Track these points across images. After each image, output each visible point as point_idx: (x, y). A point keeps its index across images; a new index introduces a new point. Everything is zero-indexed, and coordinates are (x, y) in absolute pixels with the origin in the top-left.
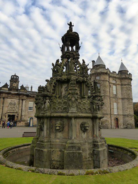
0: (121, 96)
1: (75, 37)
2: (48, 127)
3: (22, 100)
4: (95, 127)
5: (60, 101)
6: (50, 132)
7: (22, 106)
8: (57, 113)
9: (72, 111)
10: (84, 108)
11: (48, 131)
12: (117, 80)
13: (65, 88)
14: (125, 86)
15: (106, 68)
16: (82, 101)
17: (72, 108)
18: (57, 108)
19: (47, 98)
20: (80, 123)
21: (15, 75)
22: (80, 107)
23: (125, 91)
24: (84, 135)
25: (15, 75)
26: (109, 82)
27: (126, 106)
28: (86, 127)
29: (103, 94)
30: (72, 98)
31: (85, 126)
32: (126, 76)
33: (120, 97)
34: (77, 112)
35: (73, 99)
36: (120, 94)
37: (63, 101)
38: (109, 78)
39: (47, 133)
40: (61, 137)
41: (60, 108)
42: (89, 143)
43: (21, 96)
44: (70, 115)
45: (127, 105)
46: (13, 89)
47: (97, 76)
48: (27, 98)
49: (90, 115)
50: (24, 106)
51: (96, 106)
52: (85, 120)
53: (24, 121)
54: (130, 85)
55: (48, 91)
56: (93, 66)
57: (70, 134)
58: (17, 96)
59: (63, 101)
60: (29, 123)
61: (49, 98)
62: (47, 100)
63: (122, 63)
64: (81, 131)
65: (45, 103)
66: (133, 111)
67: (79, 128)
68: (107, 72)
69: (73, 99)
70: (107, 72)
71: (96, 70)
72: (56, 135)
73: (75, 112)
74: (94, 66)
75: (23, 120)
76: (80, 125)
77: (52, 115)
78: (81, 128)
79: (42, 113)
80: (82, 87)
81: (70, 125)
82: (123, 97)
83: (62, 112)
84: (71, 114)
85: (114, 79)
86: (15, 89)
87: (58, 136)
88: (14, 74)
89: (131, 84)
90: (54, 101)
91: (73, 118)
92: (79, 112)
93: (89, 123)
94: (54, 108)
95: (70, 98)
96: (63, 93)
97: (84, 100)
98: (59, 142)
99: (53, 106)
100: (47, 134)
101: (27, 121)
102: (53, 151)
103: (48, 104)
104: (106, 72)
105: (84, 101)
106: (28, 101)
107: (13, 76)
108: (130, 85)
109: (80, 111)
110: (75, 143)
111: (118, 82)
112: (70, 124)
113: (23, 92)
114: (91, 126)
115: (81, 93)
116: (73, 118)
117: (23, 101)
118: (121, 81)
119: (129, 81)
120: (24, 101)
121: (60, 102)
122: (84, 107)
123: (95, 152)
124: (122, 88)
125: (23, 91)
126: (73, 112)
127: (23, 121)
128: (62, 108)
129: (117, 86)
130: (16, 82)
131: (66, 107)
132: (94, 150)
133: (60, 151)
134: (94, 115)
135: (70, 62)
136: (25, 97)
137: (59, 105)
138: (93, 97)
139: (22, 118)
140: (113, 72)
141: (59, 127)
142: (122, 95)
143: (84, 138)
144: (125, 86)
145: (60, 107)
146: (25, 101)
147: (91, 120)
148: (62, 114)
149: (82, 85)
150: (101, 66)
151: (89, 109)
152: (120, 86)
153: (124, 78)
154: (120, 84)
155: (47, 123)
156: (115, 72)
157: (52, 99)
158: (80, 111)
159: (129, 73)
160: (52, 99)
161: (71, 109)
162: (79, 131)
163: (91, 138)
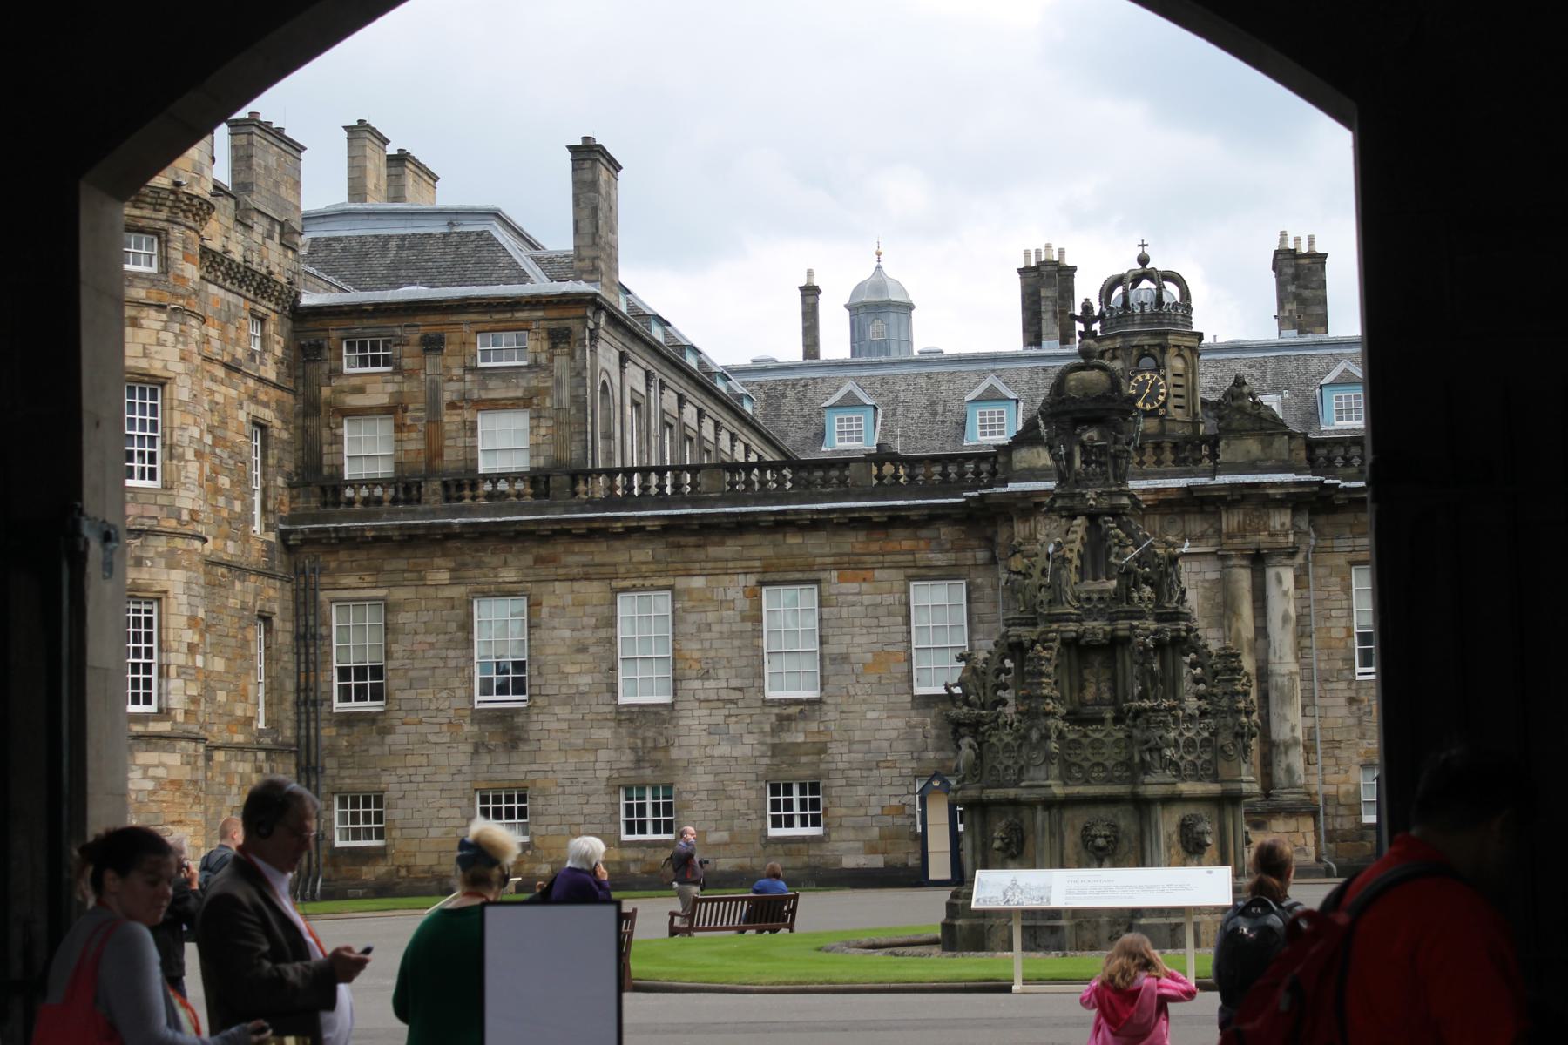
1: (1091, 406)
2: (978, 843)
3: (1258, 561)
4: (1148, 835)
7: (1262, 631)
8: (1000, 786)
9: (1032, 780)
10: (1098, 764)
16: (1086, 735)
18: (1001, 768)
19: (962, 730)
20: (1079, 825)
21: (1143, 260)
22: (1077, 760)
25: (1143, 260)
28: (1096, 836)
31: (1093, 832)
43: (1231, 521)
44: (1024, 794)
46: (1141, 449)
48: (1320, 534)
50: (1282, 639)
51: (1141, 752)
52: (1103, 812)
53: (1307, 809)
58: (1196, 525)
60: (1370, 826)
61: (973, 730)
62: (963, 737)
67: (1076, 845)
75: (1289, 798)
76: (1078, 833)
77: (984, 797)
80: (1119, 665)
84: (1029, 791)
86: (1158, 447)
88: (1129, 264)
90: (994, 740)
91: (1039, 807)
92: (1078, 779)
95: (1022, 731)
97: (1097, 730)
101: (1355, 808)
102: (992, 926)
105: (1098, 736)
106: (1341, 560)
107: (1118, 281)
109: (1079, 775)
113: (1253, 467)
114: (1133, 836)
115: (1114, 690)
116: (1039, 807)
117: (1271, 573)
120: (1282, 579)
122: (1098, 759)
125: (1252, 446)
126: (1036, 783)
127: (1292, 812)
130: (1163, 349)
136: (1280, 520)
137: (1007, 755)
139: (1279, 774)
141: (1002, 839)
146: (1288, 576)
147: (1130, 808)
149: (1118, 655)
151: (1122, 763)
157: (983, 734)
158: (1079, 775)
160: (983, 734)
161: (1028, 771)
162: (1078, 854)
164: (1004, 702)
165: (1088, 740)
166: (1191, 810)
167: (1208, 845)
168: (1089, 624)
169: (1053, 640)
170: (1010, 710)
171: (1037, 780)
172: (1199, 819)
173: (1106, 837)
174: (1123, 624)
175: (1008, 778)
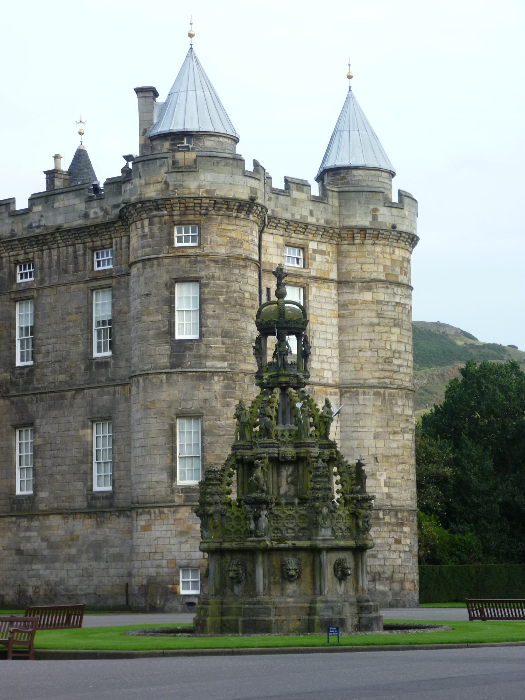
0: (335, 367)
5: (292, 513)
6: (270, 583)
9: (323, 536)
11: (267, 582)
12: (313, 246)
13: (288, 476)
14: (369, 289)
15: (249, 167)
17: (323, 530)
18: (283, 529)
23: (363, 333)
24: (341, 589)
26: (258, 264)
27: (370, 442)
29: (224, 359)
30: (322, 508)
32: (375, 218)
33: (329, 377)
34: (333, 538)
35: (325, 511)
36: (328, 352)
37: (297, 512)
38: (261, 232)
39: (264, 584)
40: (295, 592)
41: (290, 528)
42: (351, 604)
45: (376, 437)
47: (180, 223)
49: (351, 543)
54: (399, 285)
55: (263, 491)
56: (144, 132)
57: (318, 583)
59: (297, 512)
63: (349, 98)
64: (336, 579)
65: (257, 518)
66: (413, 477)
68: (253, 199)
69: (325, 511)
70: (253, 199)
71: (172, 179)
72: (282, 589)
73: (328, 537)
74: (152, 139)
76: (333, 566)
78: (335, 570)
79: (252, 541)
81: (317, 565)
82: (347, 376)
83: (296, 538)
85: (296, 238)
87: (289, 591)
89: (406, 273)
90: (276, 512)
91: (325, 552)
93: (349, 559)
94: (277, 529)
96: (284, 489)
98: (294, 602)
99: (272, 524)
100: (264, 589)
103: (264, 522)
104: (244, 195)
108: (399, 285)
110: (331, 602)
111: (318, 257)
112: (317, 562)
116: (325, 552)
118: (340, 253)
119: (399, 253)
121: (290, 515)
123: (363, 622)
124: (342, 306)
128: (297, 529)
129: (313, 290)
131: (305, 525)
132: (360, 618)
133: (300, 620)
134: (360, 543)
135: (302, 411)
137: (288, 521)
138: (358, 500)
140: (287, 181)
142: (342, 361)
143: (340, 593)
144: (368, 296)
145: (291, 526)
148: (299, 543)
150: (208, 143)
152: (334, 292)
153: (363, 230)
154: (334, 275)
155: (263, 563)
156: (303, 185)
159: (401, 194)
161: (321, 531)
162: (332, 579)
163: (352, 593)
164: (229, 493)
165: (285, 515)
166: (341, 555)
167: (349, 575)
168: (283, 449)
169: (265, 458)
170: (233, 497)
171: (326, 536)
172: (344, 560)
173: (295, 569)
174: (302, 450)
175: (287, 535)
